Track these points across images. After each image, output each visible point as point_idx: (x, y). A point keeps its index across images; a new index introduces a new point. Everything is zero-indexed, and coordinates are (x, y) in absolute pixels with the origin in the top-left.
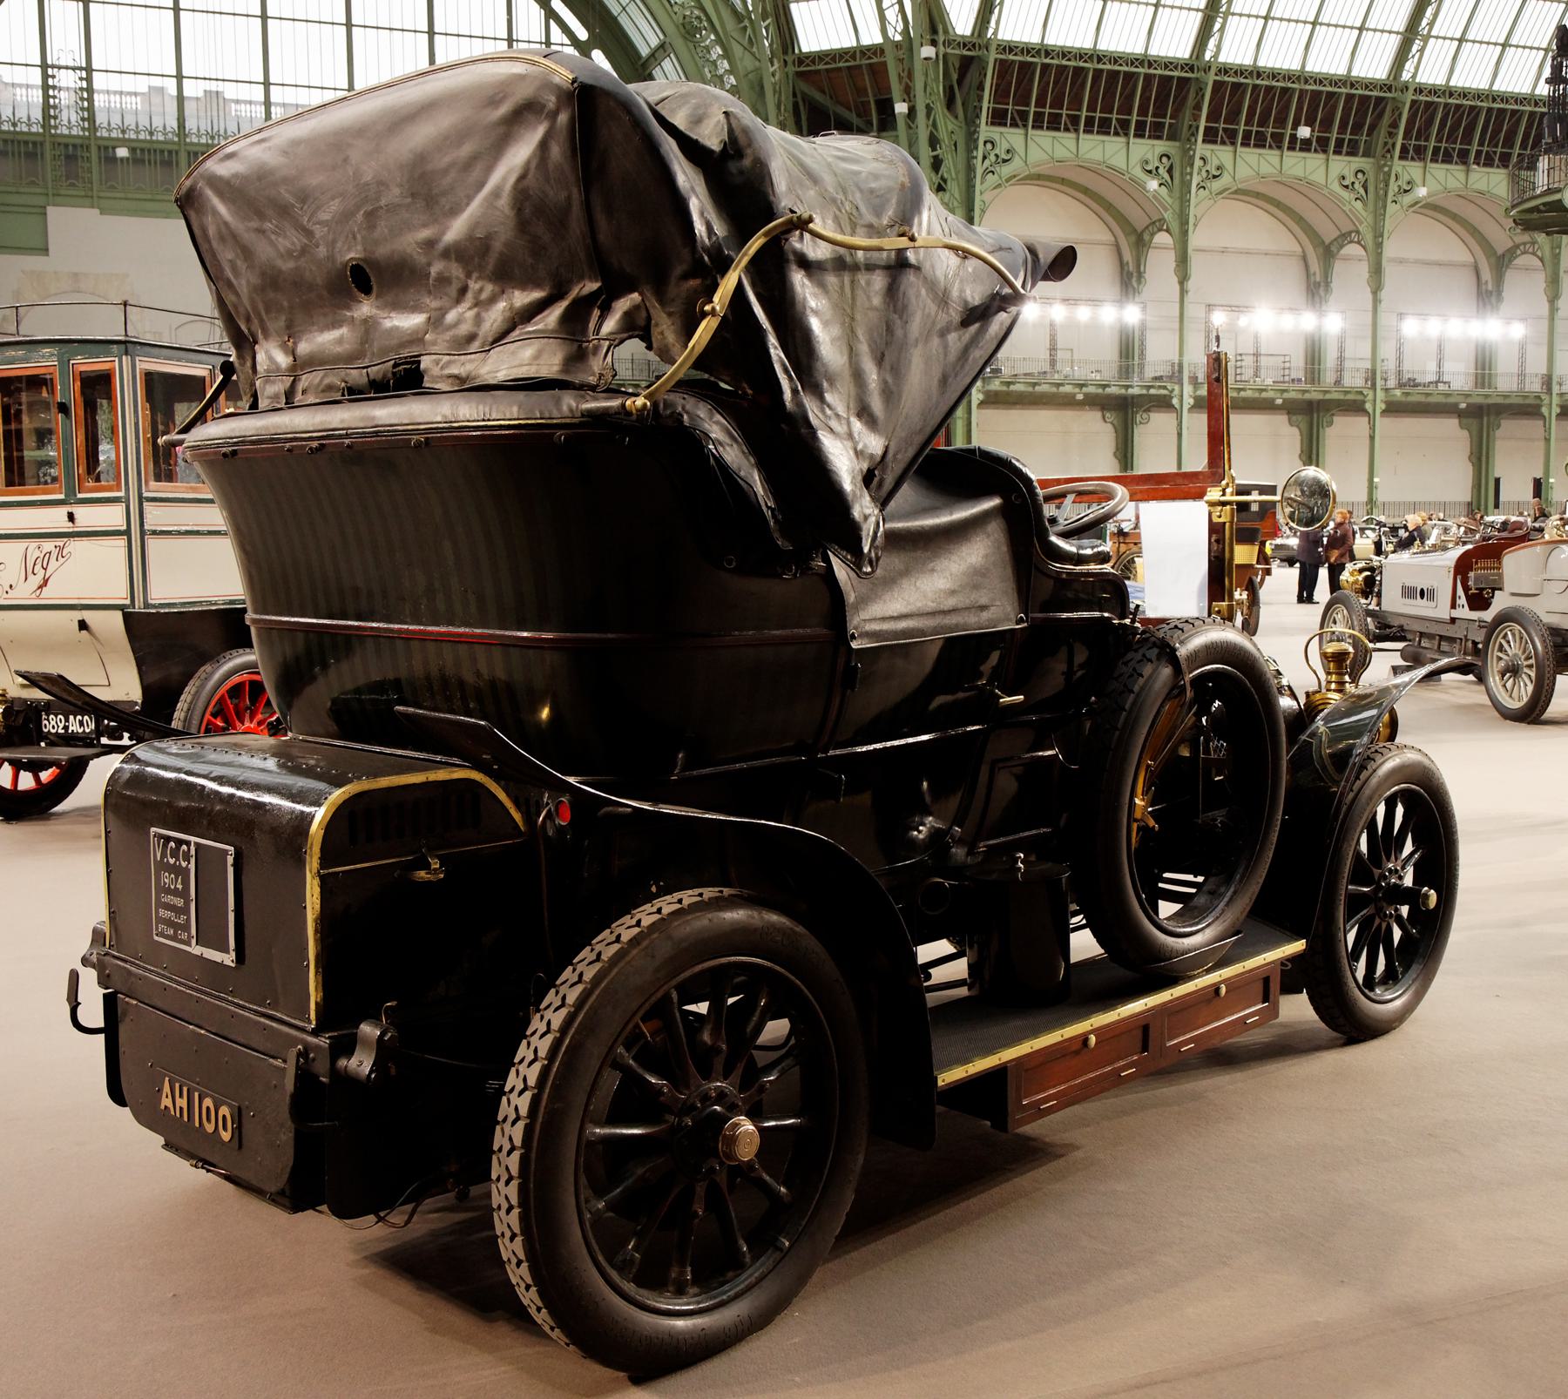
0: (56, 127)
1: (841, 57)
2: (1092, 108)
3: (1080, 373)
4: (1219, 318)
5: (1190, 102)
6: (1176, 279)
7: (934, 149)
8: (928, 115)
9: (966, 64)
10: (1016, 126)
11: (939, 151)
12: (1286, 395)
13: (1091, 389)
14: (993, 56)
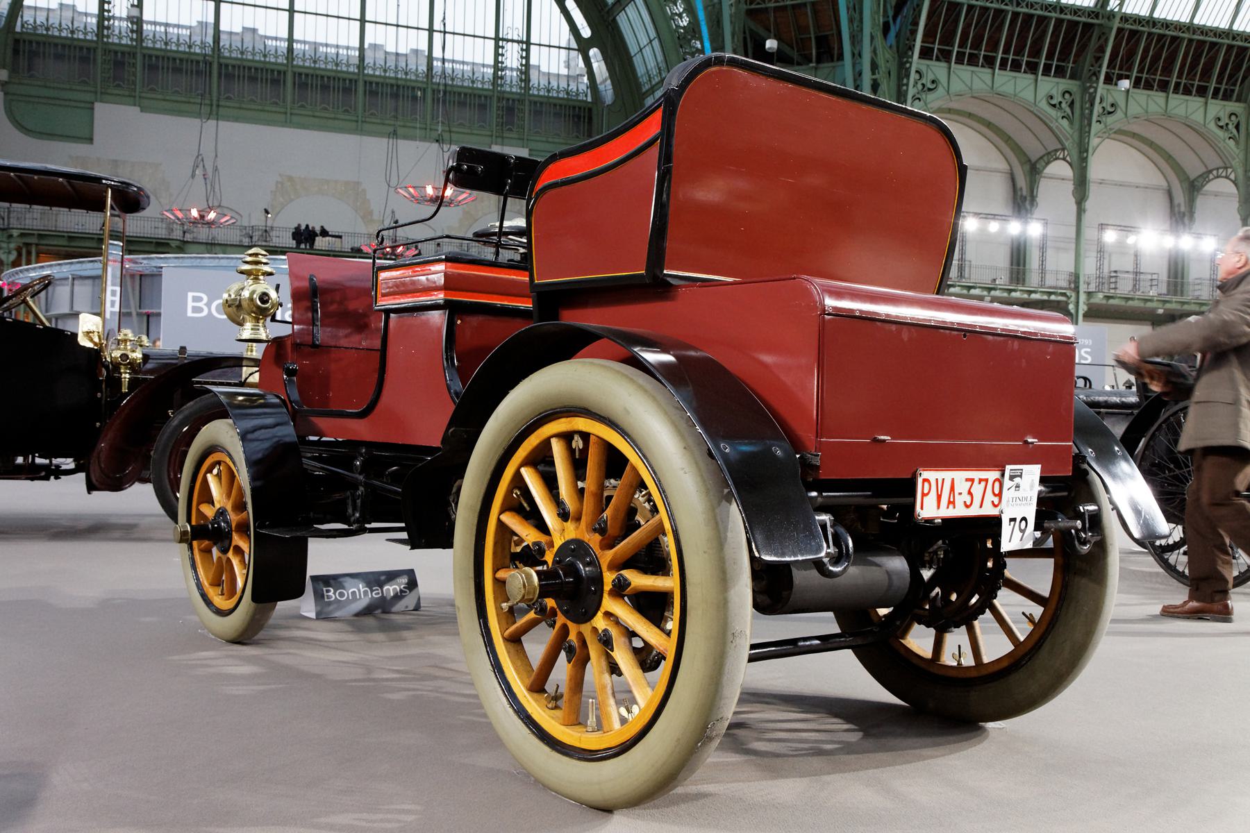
0: (108, 37)
2: (1006, 51)
3: (986, 279)
4: (1110, 236)
5: (1093, 44)
6: (1073, 200)
7: (873, 73)
11: (877, 76)
12: (1168, 306)
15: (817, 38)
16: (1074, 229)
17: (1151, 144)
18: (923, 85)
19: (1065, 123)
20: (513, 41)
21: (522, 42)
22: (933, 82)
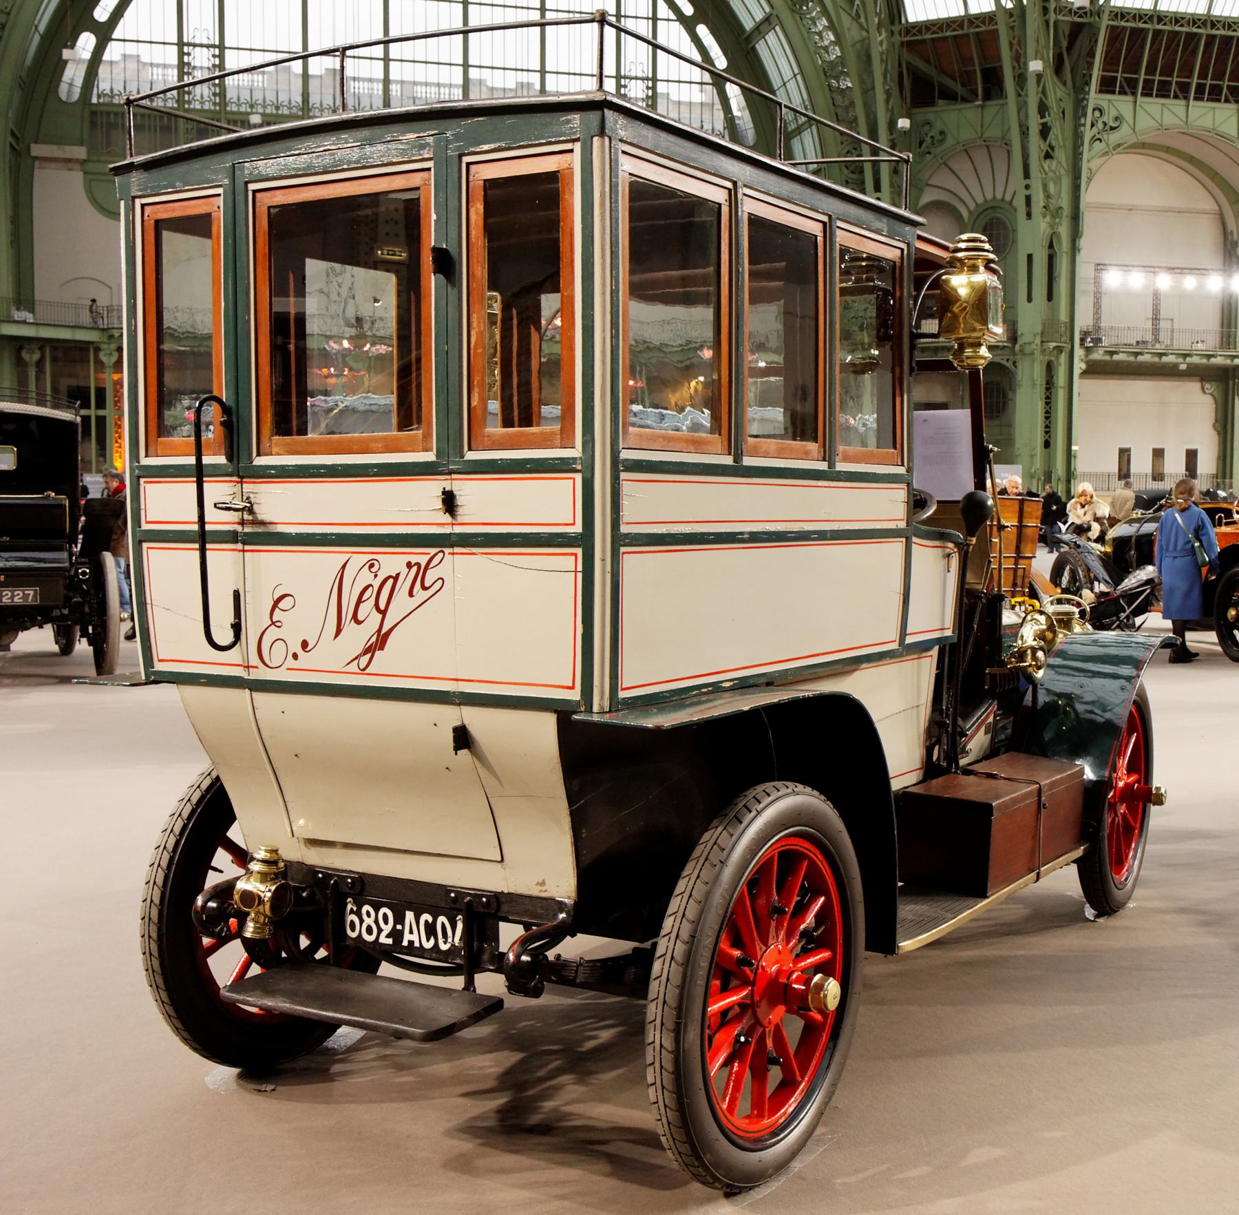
0: (189, 102)
1: (948, 26)
2: (1203, 75)
3: (1182, 343)
7: (1043, 117)
8: (1038, 82)
9: (1077, 31)
10: (1125, 93)
11: (1047, 119)
13: (1195, 360)
14: (1105, 22)
15: (983, 71)
18: (1105, 124)
20: (636, 78)
21: (647, 79)
22: (1116, 119)
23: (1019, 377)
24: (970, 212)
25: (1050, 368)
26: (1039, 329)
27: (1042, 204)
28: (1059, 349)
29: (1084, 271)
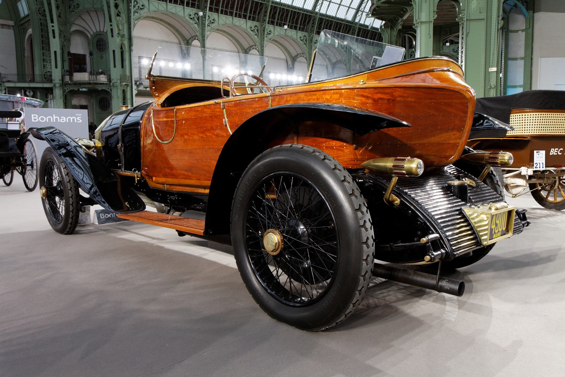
16: (202, 66)
17: (231, 35)
19: (196, 25)
22: (142, 6)
23: (113, 95)
24: (91, 35)
25: (124, 92)
26: (119, 78)
27: (117, 32)
28: (127, 85)
29: (135, 60)
